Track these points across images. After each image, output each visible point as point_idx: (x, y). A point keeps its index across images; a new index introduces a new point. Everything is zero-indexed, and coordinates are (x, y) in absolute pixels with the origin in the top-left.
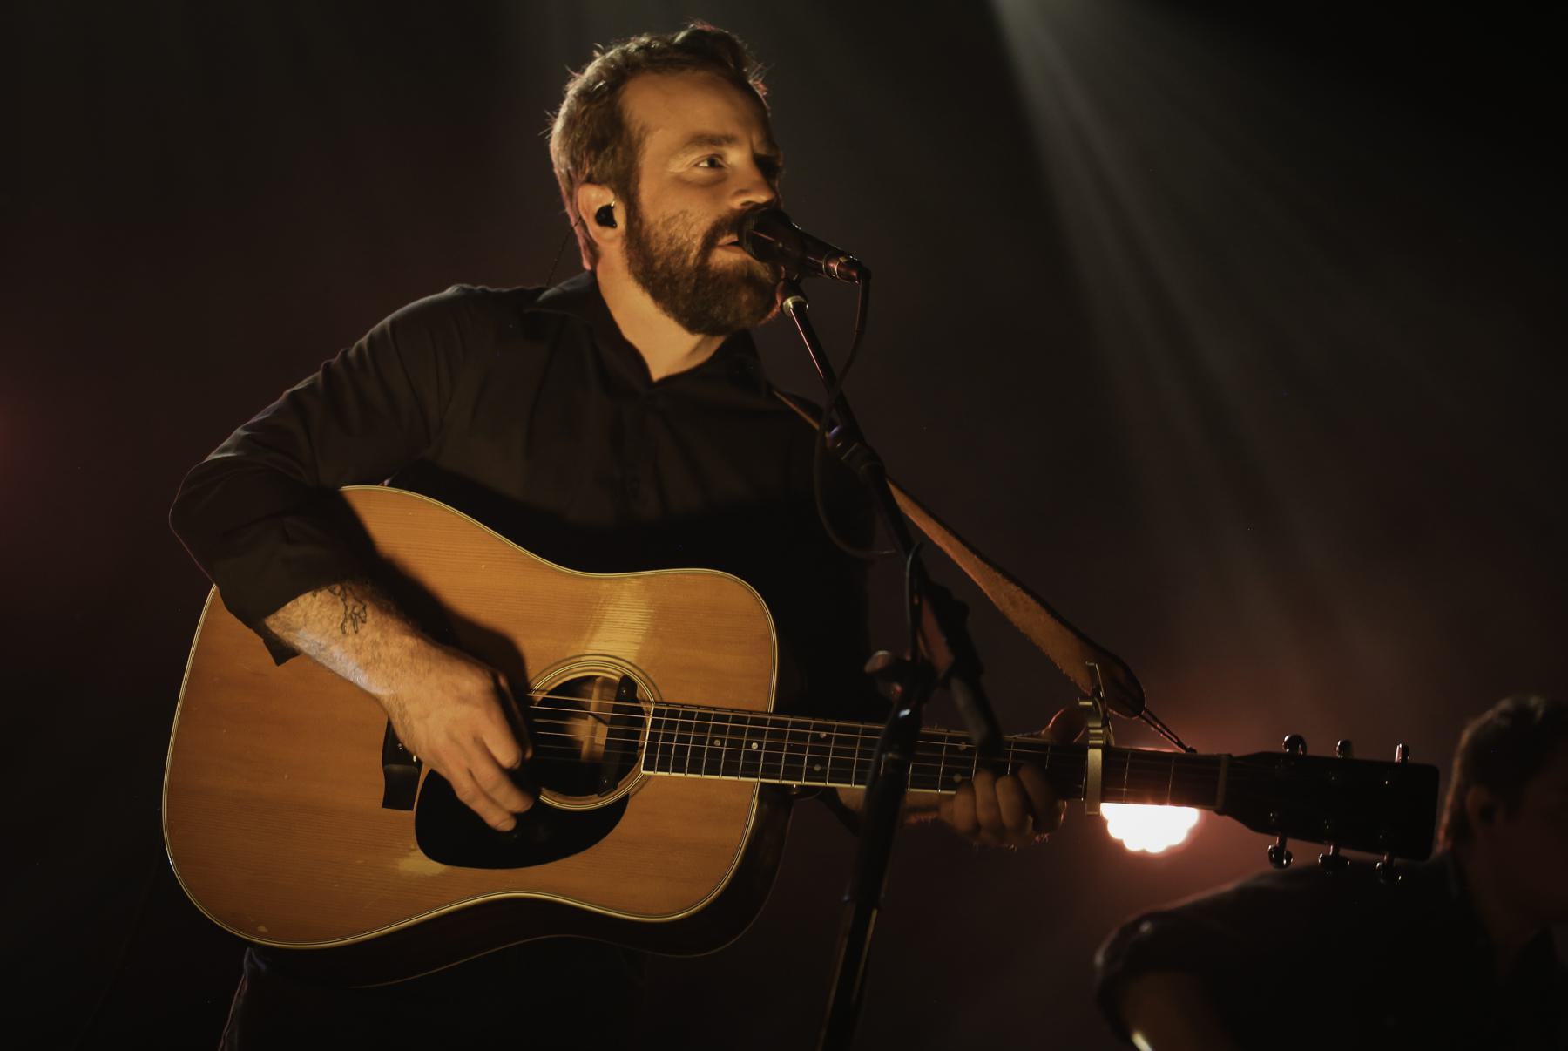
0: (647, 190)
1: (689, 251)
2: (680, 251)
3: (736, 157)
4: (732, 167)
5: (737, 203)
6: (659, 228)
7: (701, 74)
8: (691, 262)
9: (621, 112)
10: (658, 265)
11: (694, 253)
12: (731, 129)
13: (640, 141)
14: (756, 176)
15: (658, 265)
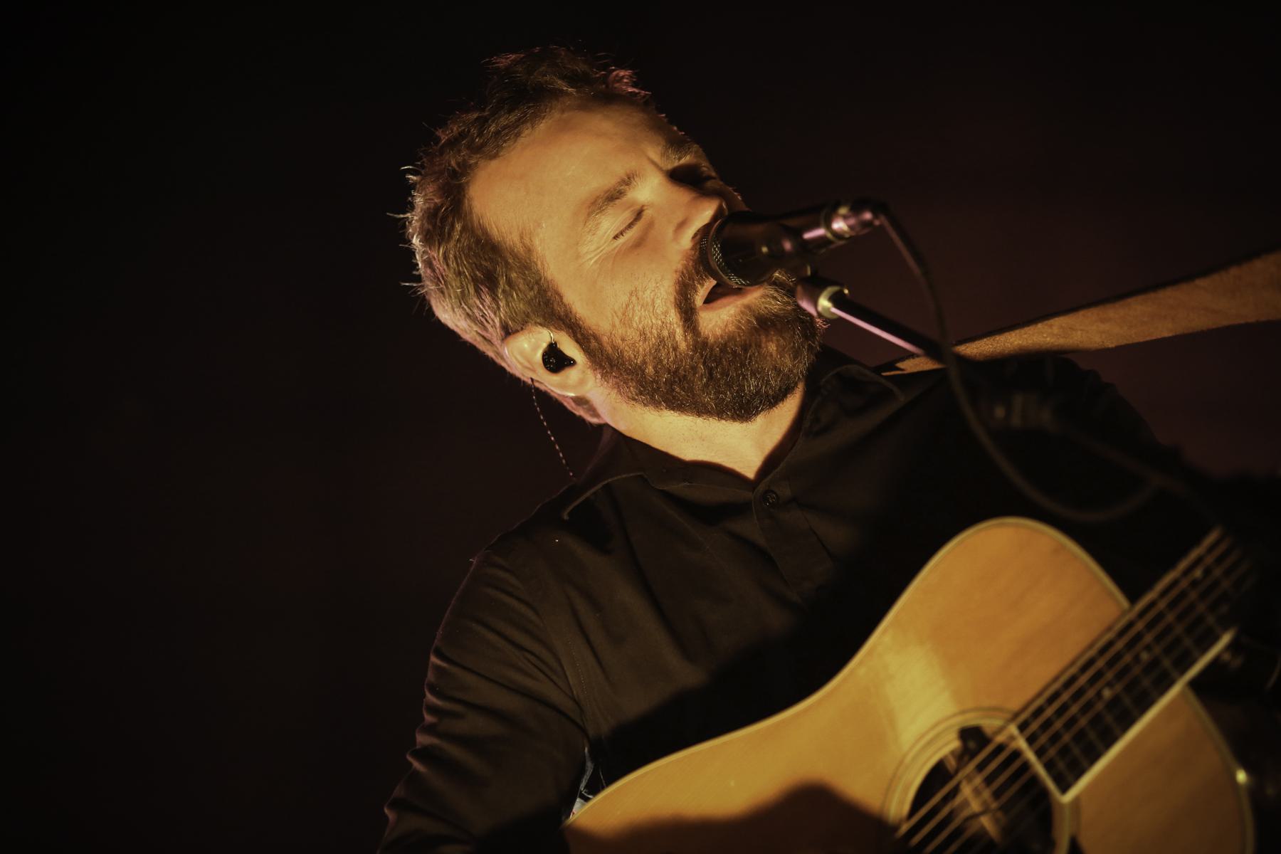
0: (576, 300)
1: (672, 335)
2: (662, 340)
3: (651, 189)
4: (651, 205)
5: (686, 240)
6: (620, 331)
7: (542, 126)
8: (683, 346)
9: (485, 233)
10: (650, 370)
11: (679, 332)
12: (619, 168)
13: (529, 250)
14: (682, 196)
15: (650, 370)
